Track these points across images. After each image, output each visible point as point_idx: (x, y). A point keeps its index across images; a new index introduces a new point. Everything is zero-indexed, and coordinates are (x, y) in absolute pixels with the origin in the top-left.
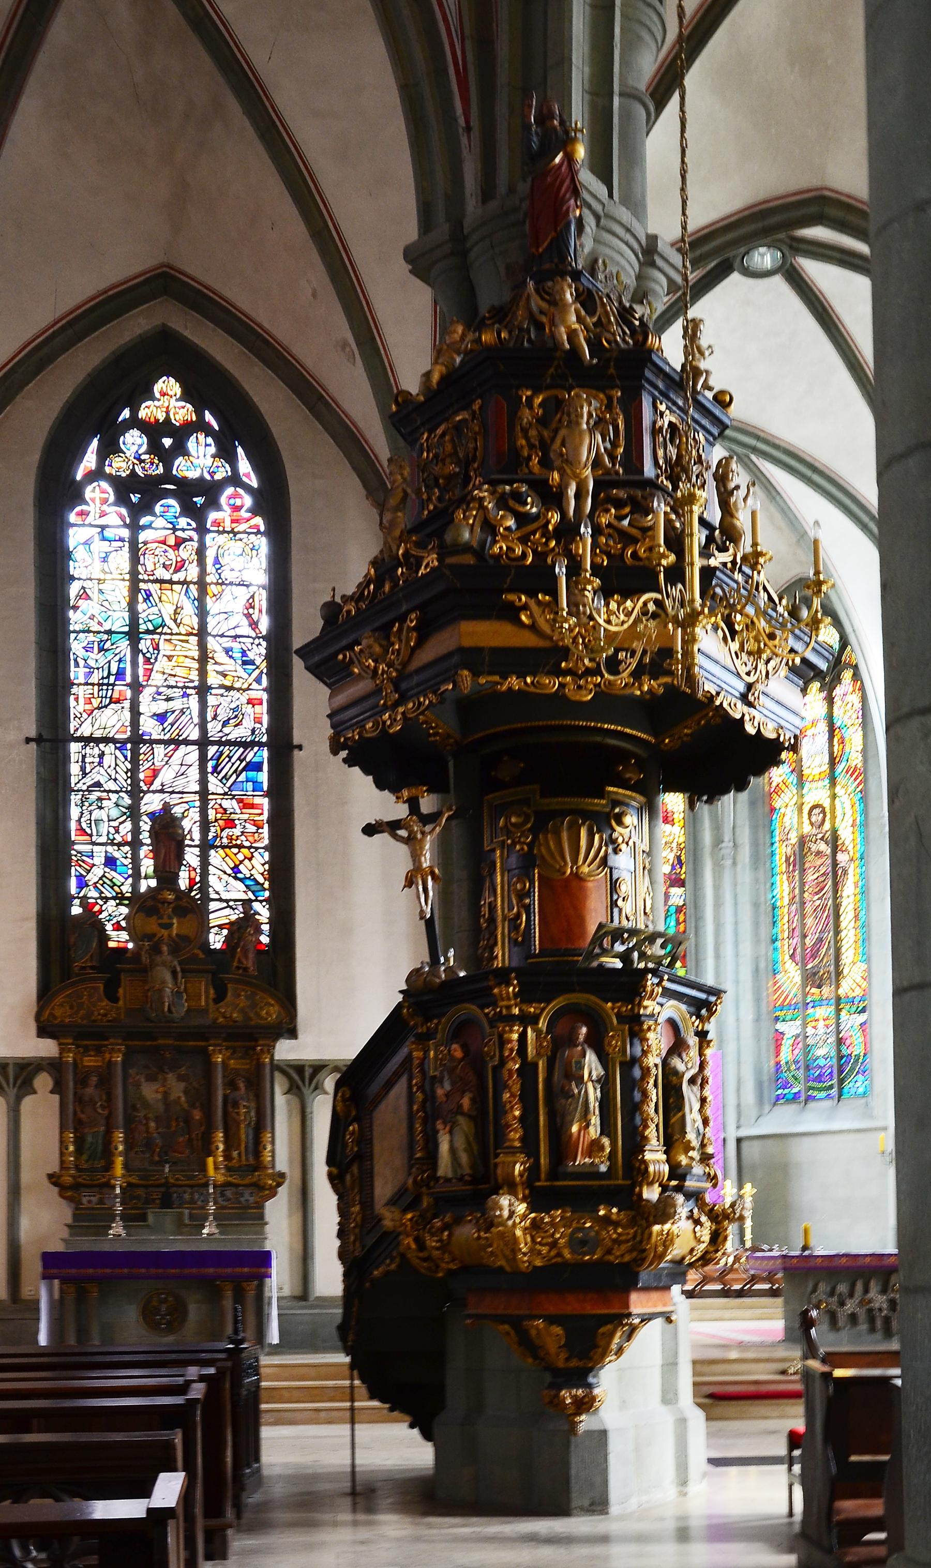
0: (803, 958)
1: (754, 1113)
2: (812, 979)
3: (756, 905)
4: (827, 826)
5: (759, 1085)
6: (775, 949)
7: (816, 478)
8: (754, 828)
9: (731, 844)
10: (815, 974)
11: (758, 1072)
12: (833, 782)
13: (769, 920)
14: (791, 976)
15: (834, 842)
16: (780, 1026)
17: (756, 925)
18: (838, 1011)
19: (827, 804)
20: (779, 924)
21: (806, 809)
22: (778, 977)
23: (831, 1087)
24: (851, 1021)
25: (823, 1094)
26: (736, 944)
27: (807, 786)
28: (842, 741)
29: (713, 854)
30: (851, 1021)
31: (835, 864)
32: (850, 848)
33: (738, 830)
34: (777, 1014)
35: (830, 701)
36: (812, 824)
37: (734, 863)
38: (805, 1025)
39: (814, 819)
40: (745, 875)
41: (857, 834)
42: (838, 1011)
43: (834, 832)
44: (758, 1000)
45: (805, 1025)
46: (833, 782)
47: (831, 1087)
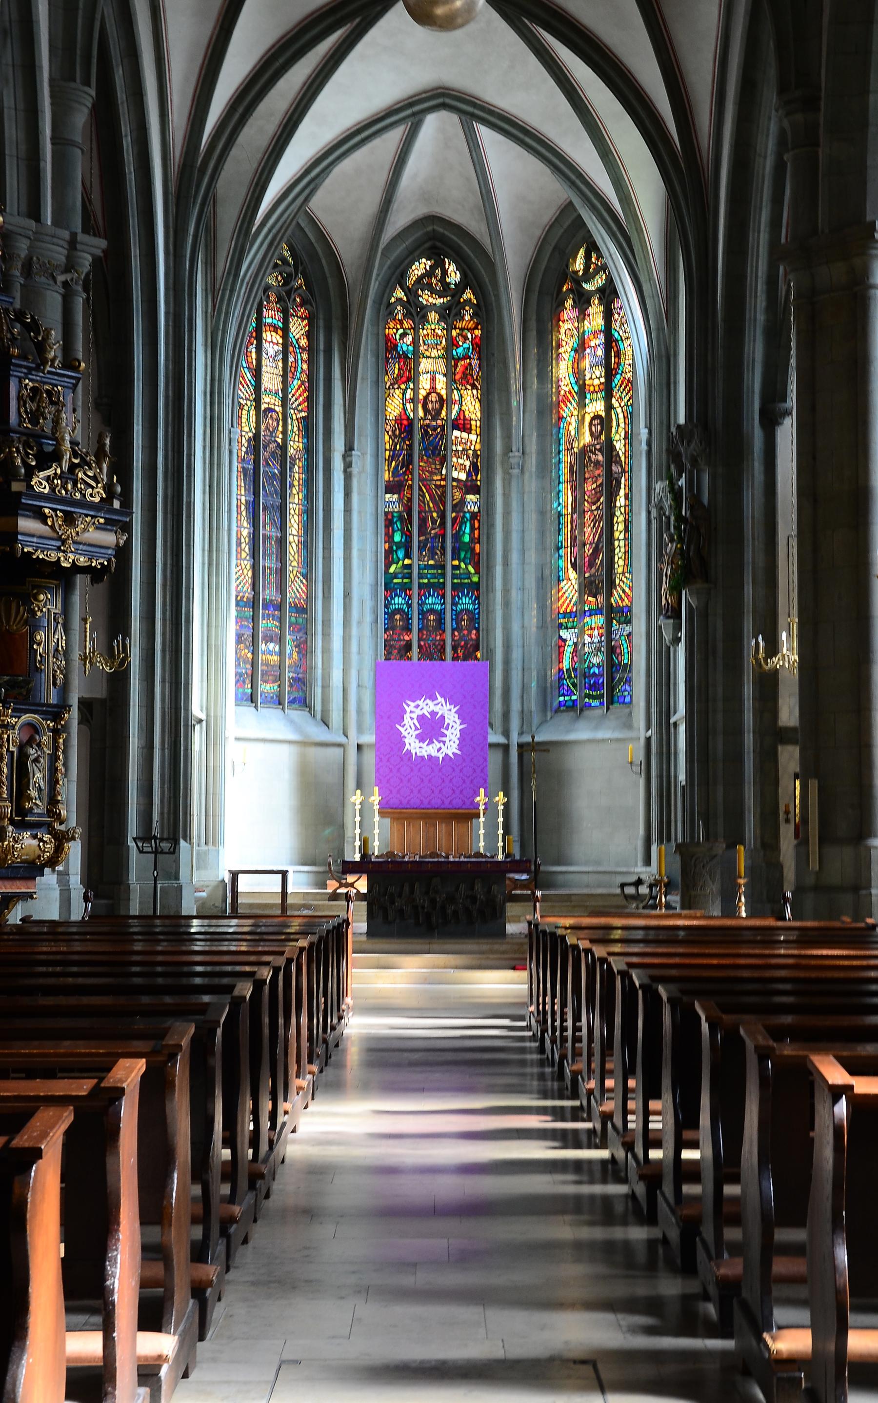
1: (536, 720)
3: (542, 513)
5: (543, 691)
6: (560, 557)
8: (542, 437)
9: (520, 454)
11: (543, 677)
13: (554, 528)
16: (564, 634)
17: (542, 533)
20: (563, 532)
22: (562, 584)
26: (523, 551)
29: (502, 463)
33: (526, 439)
34: (561, 621)
37: (522, 471)
40: (531, 484)
44: (542, 607)
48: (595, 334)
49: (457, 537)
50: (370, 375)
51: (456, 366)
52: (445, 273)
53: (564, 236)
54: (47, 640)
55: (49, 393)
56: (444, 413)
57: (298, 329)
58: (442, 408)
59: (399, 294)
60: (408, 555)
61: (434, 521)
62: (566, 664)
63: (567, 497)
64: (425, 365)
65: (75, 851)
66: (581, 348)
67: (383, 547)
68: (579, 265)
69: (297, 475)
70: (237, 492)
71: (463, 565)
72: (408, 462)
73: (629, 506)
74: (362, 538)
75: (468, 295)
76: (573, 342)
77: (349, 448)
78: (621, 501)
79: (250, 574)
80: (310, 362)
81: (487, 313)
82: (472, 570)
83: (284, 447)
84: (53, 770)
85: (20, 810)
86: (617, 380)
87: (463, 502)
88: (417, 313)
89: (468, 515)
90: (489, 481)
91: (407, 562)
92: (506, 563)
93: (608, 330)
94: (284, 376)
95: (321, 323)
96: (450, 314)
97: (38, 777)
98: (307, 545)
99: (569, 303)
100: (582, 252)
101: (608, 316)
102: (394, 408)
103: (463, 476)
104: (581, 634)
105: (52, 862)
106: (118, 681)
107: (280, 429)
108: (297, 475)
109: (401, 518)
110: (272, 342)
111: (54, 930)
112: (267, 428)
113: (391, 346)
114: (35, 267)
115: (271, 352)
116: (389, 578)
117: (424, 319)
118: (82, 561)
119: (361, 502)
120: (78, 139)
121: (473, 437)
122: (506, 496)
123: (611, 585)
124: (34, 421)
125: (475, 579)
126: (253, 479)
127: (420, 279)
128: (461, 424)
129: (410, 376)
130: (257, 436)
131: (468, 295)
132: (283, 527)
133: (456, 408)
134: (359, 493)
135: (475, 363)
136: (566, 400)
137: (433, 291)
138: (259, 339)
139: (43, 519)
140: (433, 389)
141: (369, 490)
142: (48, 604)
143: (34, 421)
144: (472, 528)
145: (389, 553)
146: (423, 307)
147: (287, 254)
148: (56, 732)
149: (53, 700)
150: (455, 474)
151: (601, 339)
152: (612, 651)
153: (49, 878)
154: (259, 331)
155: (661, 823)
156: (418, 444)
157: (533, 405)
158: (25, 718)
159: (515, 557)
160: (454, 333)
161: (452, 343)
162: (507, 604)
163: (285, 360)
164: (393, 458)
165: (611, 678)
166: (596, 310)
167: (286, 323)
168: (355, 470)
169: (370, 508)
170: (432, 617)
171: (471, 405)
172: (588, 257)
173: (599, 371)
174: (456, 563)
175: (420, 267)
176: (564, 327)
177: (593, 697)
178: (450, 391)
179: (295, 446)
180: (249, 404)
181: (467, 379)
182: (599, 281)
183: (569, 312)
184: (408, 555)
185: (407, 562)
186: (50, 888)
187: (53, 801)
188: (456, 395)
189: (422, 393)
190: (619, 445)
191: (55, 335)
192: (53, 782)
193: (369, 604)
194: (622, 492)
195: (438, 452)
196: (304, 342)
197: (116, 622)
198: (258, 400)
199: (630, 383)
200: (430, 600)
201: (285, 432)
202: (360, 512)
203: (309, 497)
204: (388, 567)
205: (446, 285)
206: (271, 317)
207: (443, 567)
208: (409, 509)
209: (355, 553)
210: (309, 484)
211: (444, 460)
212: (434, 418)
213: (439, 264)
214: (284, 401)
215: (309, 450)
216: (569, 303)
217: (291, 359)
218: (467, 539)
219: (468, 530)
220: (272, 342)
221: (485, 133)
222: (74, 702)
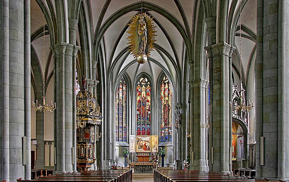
2: (165, 124)
3: (159, 114)
12: (168, 98)
14: (163, 125)
15: (169, 106)
16: (162, 131)
17: (159, 117)
18: (168, 129)
24: (170, 131)
30: (170, 131)
31: (169, 108)
40: (157, 110)
46: (168, 98)
48: (167, 89)
49: (147, 117)
50: (135, 94)
53: (162, 75)
54: (92, 134)
55: (92, 102)
57: (124, 88)
59: (139, 83)
62: (163, 135)
63: (163, 111)
64: (142, 93)
65: (96, 161)
66: (165, 90)
67: (137, 119)
68: (164, 79)
69: (124, 109)
70: (116, 111)
72: (140, 107)
73: (171, 113)
75: (149, 83)
76: (164, 90)
77: (132, 105)
78: (170, 112)
79: (118, 123)
80: (126, 93)
81: (151, 85)
83: (122, 105)
84: (93, 151)
85: (89, 156)
86: (170, 95)
88: (141, 86)
90: (152, 109)
92: (154, 121)
93: (168, 88)
94: (122, 95)
96: (146, 86)
97: (91, 152)
98: (126, 119)
99: (163, 84)
100: (165, 78)
101: (168, 86)
102: (138, 99)
103: (148, 109)
104: (165, 131)
105: (93, 163)
106: (100, 139)
108: (124, 109)
109: (139, 115)
111: (93, 171)
113: (138, 90)
114: (90, 85)
115: (121, 91)
116: (138, 123)
117: (142, 86)
118: (96, 124)
120: (95, 68)
121: (149, 103)
122: (154, 111)
123: (169, 124)
124: (90, 106)
125: (150, 123)
128: (148, 101)
129: (140, 94)
130: (119, 103)
131: (149, 83)
132: (122, 116)
133: (147, 99)
135: (150, 93)
136: (162, 98)
138: (119, 90)
139: (91, 118)
140: (144, 96)
141: (135, 111)
142: (92, 129)
143: (90, 106)
145: (137, 119)
147: (123, 78)
148: (93, 146)
149: (93, 142)
150: (147, 108)
151: (167, 89)
152: (169, 133)
153: (93, 165)
154: (119, 88)
155: (175, 157)
156: (141, 104)
157: (158, 98)
158: (90, 144)
159: (155, 120)
160: (147, 88)
161: (146, 90)
162: (154, 127)
163: (123, 93)
164: (138, 106)
165: (169, 137)
166: (167, 85)
167: (123, 87)
169: (135, 113)
171: (149, 98)
172: (166, 78)
173: (167, 94)
175: (142, 79)
176: (162, 87)
177: (166, 140)
179: (124, 105)
180: (118, 99)
181: (148, 95)
182: (167, 81)
183: (163, 85)
186: (93, 166)
187: (93, 155)
188: (147, 97)
189: (142, 97)
190: (170, 104)
191: (93, 94)
192: (93, 153)
193: (135, 127)
194: (170, 111)
195: (144, 106)
196: (125, 90)
197: (100, 131)
198: (119, 98)
199: (172, 96)
203: (126, 112)
204: (137, 121)
206: (121, 86)
207: (145, 121)
208: (140, 114)
211: (145, 106)
214: (122, 98)
216: (163, 84)
217: (123, 92)
218: (148, 117)
221: (150, 61)
222: (95, 142)
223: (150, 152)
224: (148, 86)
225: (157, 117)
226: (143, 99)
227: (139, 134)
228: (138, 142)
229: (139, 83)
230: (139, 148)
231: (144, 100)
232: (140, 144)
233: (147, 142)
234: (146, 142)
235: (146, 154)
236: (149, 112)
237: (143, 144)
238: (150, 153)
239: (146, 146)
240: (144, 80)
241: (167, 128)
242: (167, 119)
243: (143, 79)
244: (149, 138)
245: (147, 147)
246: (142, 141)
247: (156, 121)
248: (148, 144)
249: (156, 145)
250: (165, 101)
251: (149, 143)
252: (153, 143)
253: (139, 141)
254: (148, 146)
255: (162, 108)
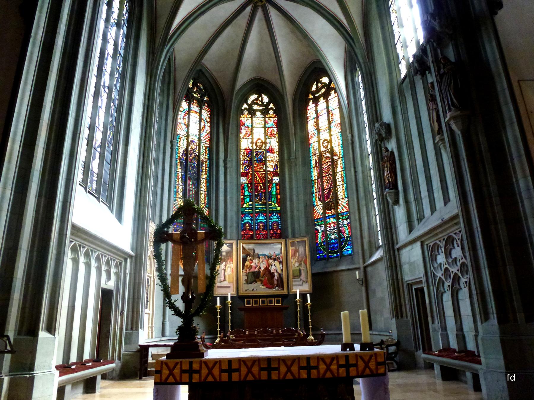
0: (324, 198)
2: (327, 207)
4: (329, 147)
7: (318, 8)
10: (328, 205)
14: (319, 209)
18: (338, 219)
19: (328, 139)
21: (321, 142)
23: (337, 252)
25: (335, 255)
27: (321, 133)
28: (332, 115)
30: (344, 223)
31: (333, 160)
32: (338, 153)
35: (327, 102)
36: (324, 147)
38: (326, 226)
39: (324, 145)
41: (340, 148)
42: (338, 219)
43: (332, 149)
45: (326, 226)
47: (337, 252)
51: (268, 130)
52: (262, 99)
56: (263, 147)
57: (205, 114)
58: (263, 145)
60: (250, 201)
61: (261, 187)
69: (205, 168)
71: (273, 204)
74: (232, 193)
75: (271, 106)
77: (226, 157)
82: (277, 205)
83: (199, 156)
87: (272, 179)
88: (252, 113)
89: (274, 184)
91: (251, 203)
95: (215, 113)
96: (265, 112)
103: (272, 170)
107: (198, 149)
108: (205, 168)
110: (194, 117)
112: (192, 148)
119: (231, 178)
125: (279, 209)
126: (185, 167)
127: (253, 101)
128: (271, 151)
131: (271, 106)
132: (198, 187)
134: (230, 175)
135: (275, 129)
137: (258, 105)
141: (234, 174)
144: (277, 189)
146: (254, 110)
161: (265, 122)
163: (200, 124)
168: (229, 165)
170: (261, 225)
171: (274, 143)
174: (270, 203)
178: (266, 139)
179: (204, 157)
184: (250, 201)
185: (251, 203)
188: (268, 140)
196: (208, 120)
200: (260, 218)
201: (199, 150)
202: (230, 183)
205: (263, 103)
209: (228, 197)
210: (210, 172)
211: (265, 164)
212: (260, 149)
213: (261, 96)
215: (210, 159)
217: (202, 124)
218: (274, 193)
219: (275, 190)
220: (194, 117)
223: (285, 292)
224: (271, 112)
225: (301, 189)
226: (257, 146)
227: (245, 237)
228: (244, 260)
229: (245, 106)
230: (248, 282)
231: (261, 146)
232: (251, 267)
233: (275, 260)
234: (271, 261)
235: (271, 302)
236: (276, 179)
237: (263, 269)
238: (284, 297)
239: (272, 275)
240: (260, 99)
241: (332, 216)
242: (329, 192)
243: (256, 96)
244: (279, 246)
245: (276, 278)
246: (257, 259)
247: (298, 200)
248: (276, 267)
249: (303, 268)
250: (319, 141)
251: (280, 262)
252: (294, 263)
253: (249, 258)
254: (276, 274)
255: (313, 164)
